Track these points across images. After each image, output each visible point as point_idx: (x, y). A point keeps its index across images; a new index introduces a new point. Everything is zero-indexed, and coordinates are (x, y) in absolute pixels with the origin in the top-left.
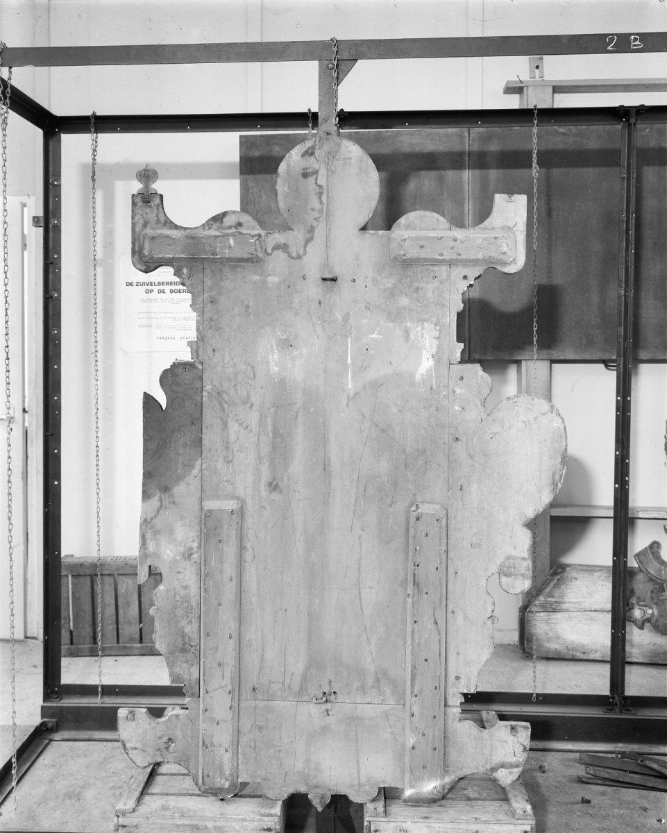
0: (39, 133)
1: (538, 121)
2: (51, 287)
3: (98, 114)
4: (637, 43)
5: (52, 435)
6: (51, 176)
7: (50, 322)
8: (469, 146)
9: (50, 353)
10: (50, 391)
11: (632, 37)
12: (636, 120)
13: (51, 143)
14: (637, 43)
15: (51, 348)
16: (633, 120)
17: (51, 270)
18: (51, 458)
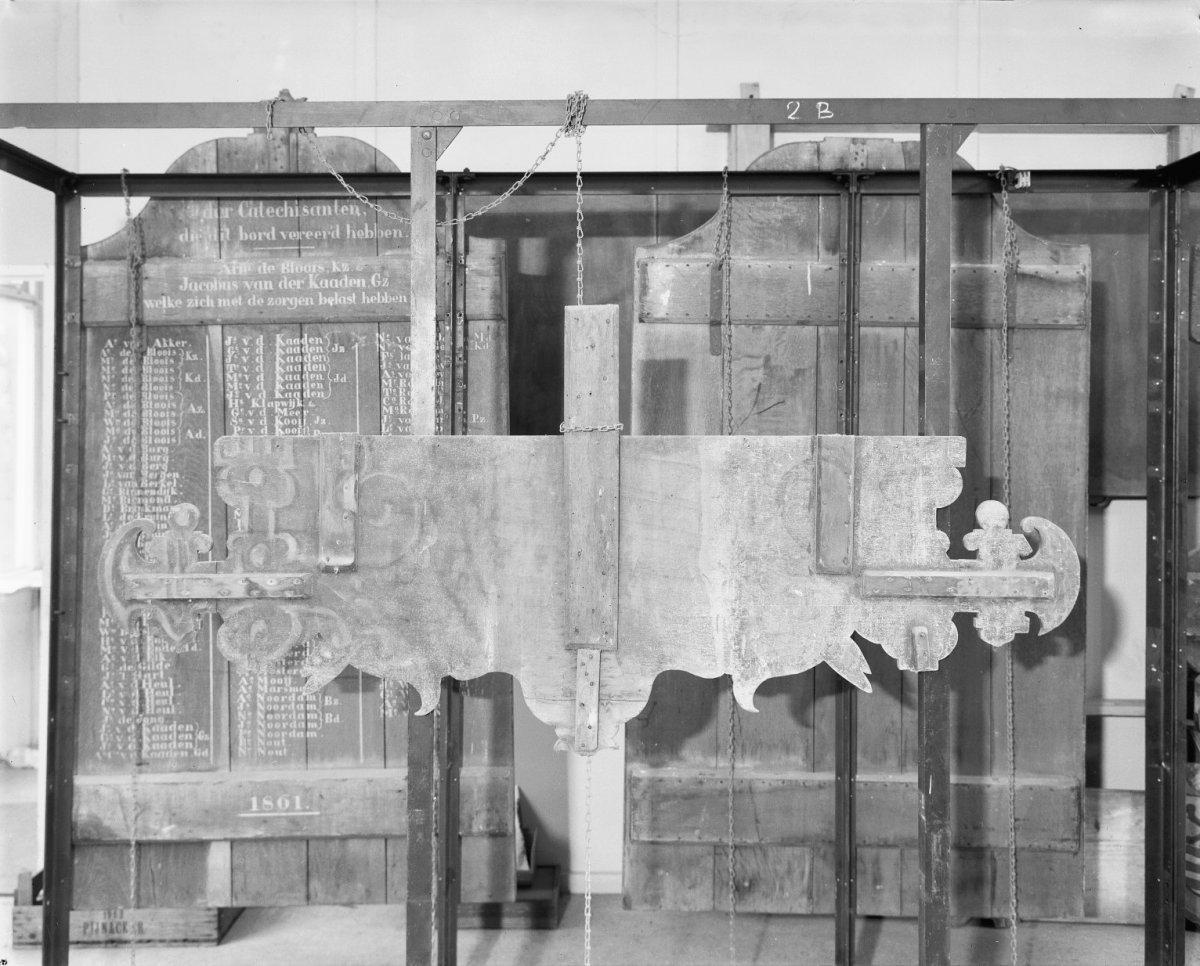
0: (48, 197)
1: (729, 188)
2: (64, 407)
3: (132, 171)
4: (826, 111)
5: (63, 613)
6: (66, 255)
7: (64, 456)
8: (658, 204)
9: (63, 499)
10: (62, 553)
11: (820, 104)
12: (858, 188)
13: (67, 210)
14: (826, 111)
15: (63, 492)
16: (853, 189)
17: (65, 383)
18: (60, 644)
